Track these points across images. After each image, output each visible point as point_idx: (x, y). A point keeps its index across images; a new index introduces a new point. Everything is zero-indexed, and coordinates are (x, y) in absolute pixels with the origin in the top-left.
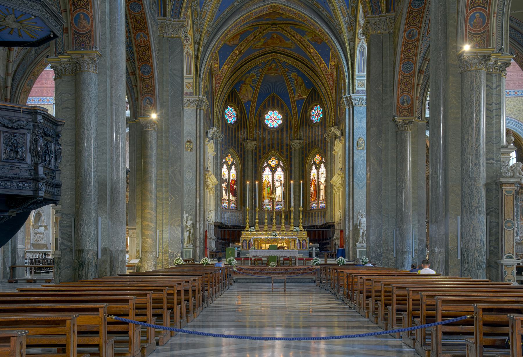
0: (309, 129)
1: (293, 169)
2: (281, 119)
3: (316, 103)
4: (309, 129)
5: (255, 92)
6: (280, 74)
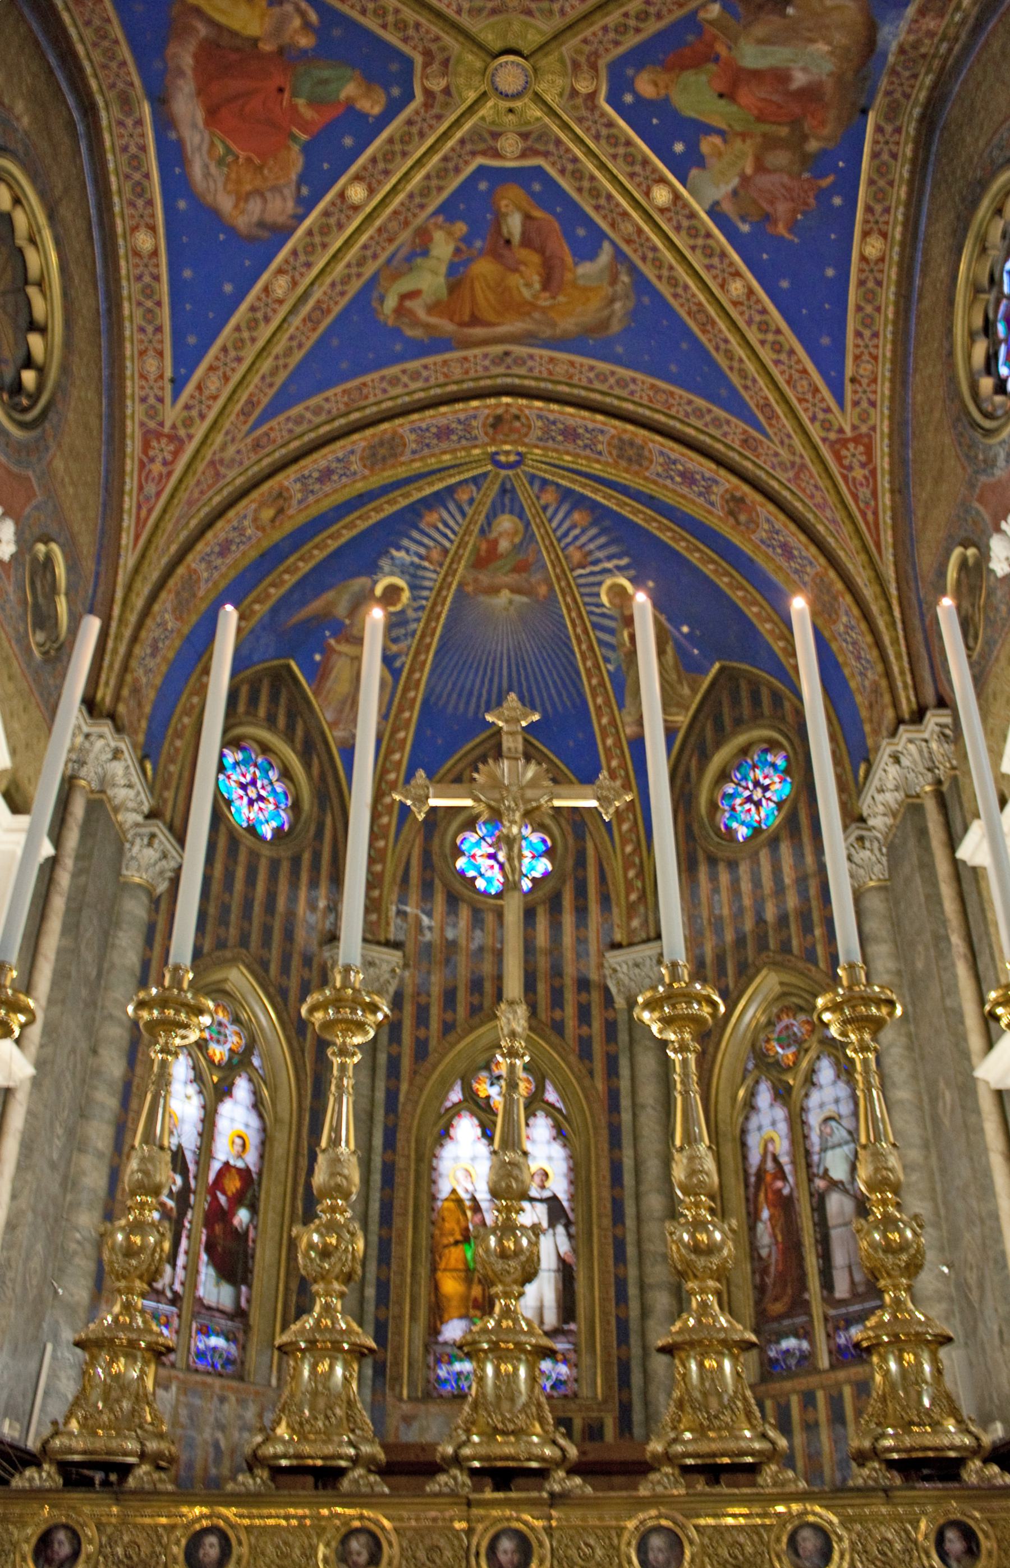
0: (714, 878)
1: (626, 1117)
2: (549, 853)
3: (741, 740)
4: (714, 878)
5: (406, 690)
6: (543, 590)
